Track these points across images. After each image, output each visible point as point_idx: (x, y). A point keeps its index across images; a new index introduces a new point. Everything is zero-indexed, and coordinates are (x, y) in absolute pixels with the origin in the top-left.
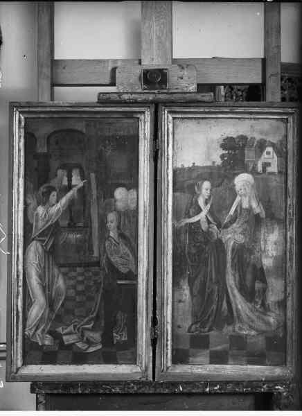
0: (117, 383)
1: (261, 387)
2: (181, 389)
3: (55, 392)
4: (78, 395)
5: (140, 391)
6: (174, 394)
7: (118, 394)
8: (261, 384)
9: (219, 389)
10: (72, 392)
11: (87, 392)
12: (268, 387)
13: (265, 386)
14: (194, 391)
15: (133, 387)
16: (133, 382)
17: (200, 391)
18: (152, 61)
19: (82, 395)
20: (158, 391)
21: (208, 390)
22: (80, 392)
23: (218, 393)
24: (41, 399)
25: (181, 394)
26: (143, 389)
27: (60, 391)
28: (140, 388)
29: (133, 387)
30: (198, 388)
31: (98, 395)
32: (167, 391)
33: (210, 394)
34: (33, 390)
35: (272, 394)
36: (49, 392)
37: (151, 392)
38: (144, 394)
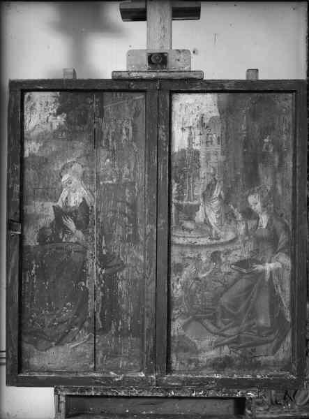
3: (74, 394)
4: (91, 396)
5: (141, 395)
6: (167, 397)
7: (123, 397)
10: (86, 393)
11: (98, 394)
12: (242, 393)
14: (183, 395)
17: (188, 395)
18: (156, 49)
20: (155, 395)
21: (194, 394)
22: (93, 394)
23: (202, 397)
24: (63, 399)
25: (173, 397)
27: (77, 393)
28: (140, 392)
29: (135, 392)
30: (186, 392)
31: (107, 397)
32: (162, 395)
33: (195, 398)
35: (245, 398)
36: (68, 394)
37: (150, 395)
38: (143, 397)
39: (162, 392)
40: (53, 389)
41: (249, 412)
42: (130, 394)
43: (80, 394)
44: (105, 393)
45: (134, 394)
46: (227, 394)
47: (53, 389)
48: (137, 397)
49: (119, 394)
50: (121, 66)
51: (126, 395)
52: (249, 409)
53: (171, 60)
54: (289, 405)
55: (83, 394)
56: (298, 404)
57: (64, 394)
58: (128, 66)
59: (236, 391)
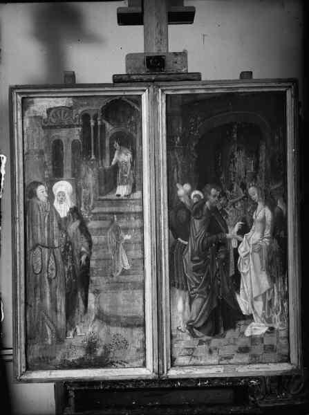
0: (132, 381)
1: (240, 382)
2: (179, 384)
5: (148, 386)
8: (239, 380)
9: (208, 384)
10: (95, 388)
13: (243, 381)
14: (189, 385)
15: (142, 384)
16: (143, 380)
18: (154, 51)
21: (199, 384)
28: (148, 384)
29: (142, 384)
32: (168, 386)
39: (169, 383)
41: (252, 399)
45: (141, 386)
46: (231, 383)
50: (122, 70)
52: (252, 396)
53: (169, 63)
54: (284, 394)
56: (292, 392)
57: (73, 389)
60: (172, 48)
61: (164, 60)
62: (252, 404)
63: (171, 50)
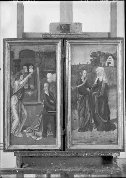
3: (24, 155)
5: (59, 155)
7: (50, 156)
11: (37, 155)
13: (110, 153)
18: (66, 22)
19: (35, 156)
21: (86, 155)
22: (34, 155)
26: (60, 154)
28: (59, 154)
32: (70, 155)
33: (87, 156)
34: (15, 155)
39: (70, 154)
40: (13, 153)
41: (115, 163)
42: (54, 155)
43: (28, 155)
44: (40, 155)
45: (55, 155)
46: (103, 154)
47: (13, 153)
48: (57, 156)
49: (48, 155)
50: (46, 30)
51: (51, 155)
53: (73, 28)
55: (29, 155)
57: (19, 155)
58: (50, 30)
59: (108, 152)
60: (75, 20)
61: (70, 26)
62: (115, 166)
63: (74, 21)
